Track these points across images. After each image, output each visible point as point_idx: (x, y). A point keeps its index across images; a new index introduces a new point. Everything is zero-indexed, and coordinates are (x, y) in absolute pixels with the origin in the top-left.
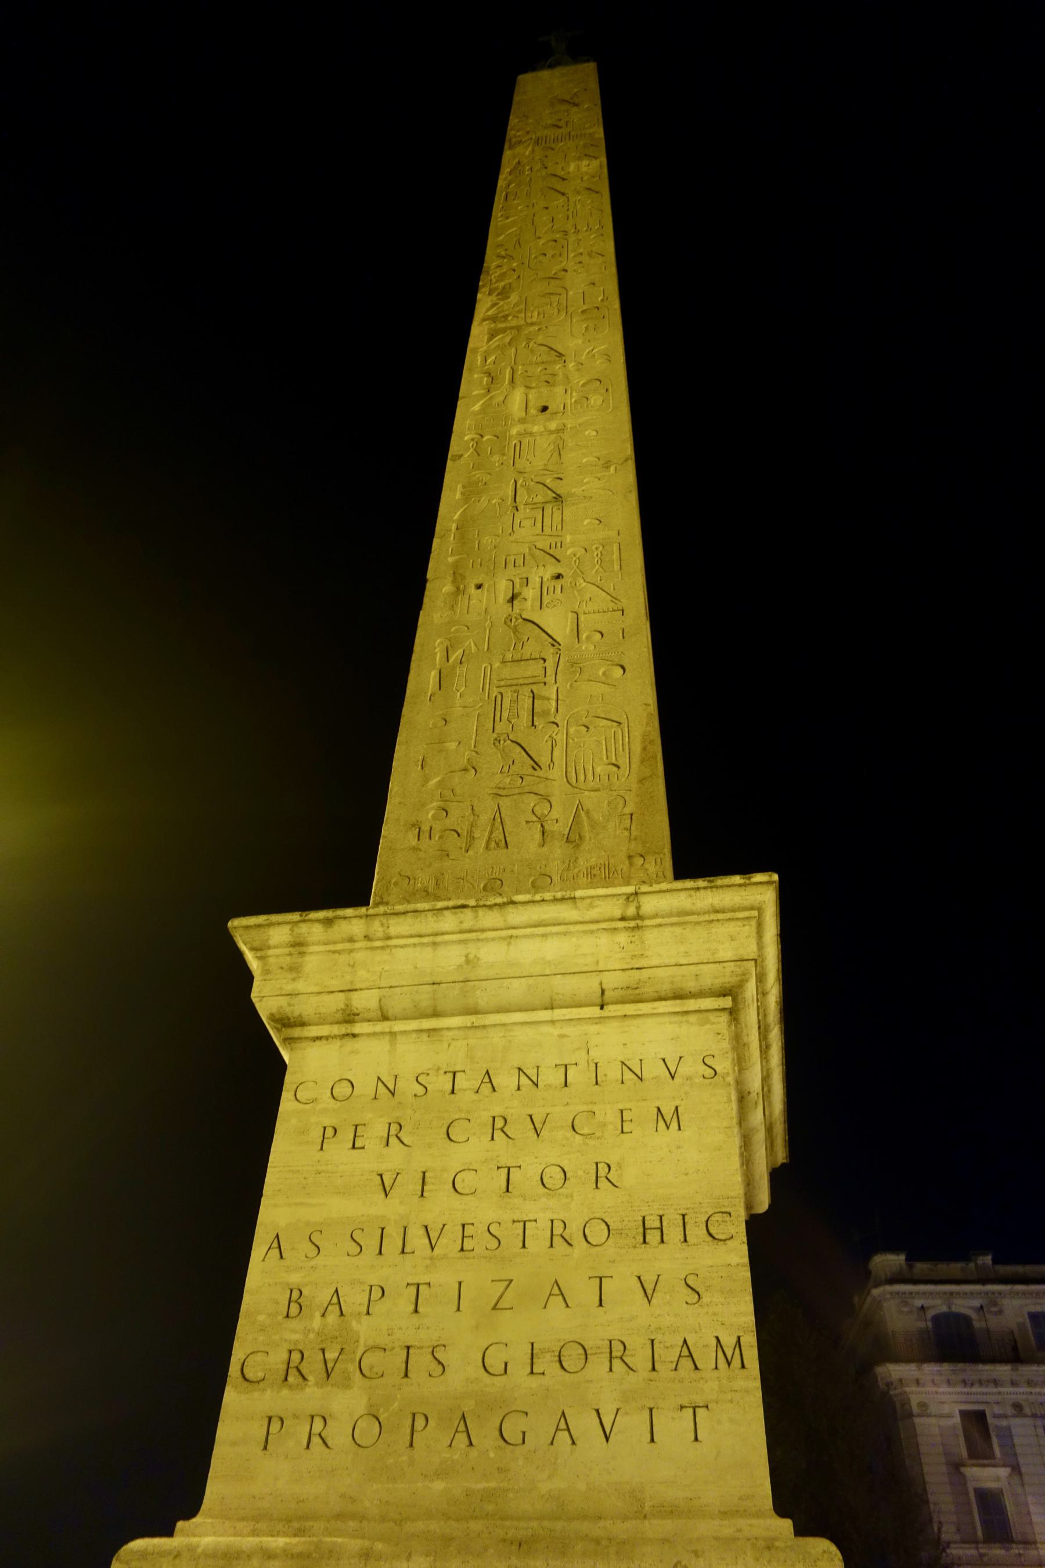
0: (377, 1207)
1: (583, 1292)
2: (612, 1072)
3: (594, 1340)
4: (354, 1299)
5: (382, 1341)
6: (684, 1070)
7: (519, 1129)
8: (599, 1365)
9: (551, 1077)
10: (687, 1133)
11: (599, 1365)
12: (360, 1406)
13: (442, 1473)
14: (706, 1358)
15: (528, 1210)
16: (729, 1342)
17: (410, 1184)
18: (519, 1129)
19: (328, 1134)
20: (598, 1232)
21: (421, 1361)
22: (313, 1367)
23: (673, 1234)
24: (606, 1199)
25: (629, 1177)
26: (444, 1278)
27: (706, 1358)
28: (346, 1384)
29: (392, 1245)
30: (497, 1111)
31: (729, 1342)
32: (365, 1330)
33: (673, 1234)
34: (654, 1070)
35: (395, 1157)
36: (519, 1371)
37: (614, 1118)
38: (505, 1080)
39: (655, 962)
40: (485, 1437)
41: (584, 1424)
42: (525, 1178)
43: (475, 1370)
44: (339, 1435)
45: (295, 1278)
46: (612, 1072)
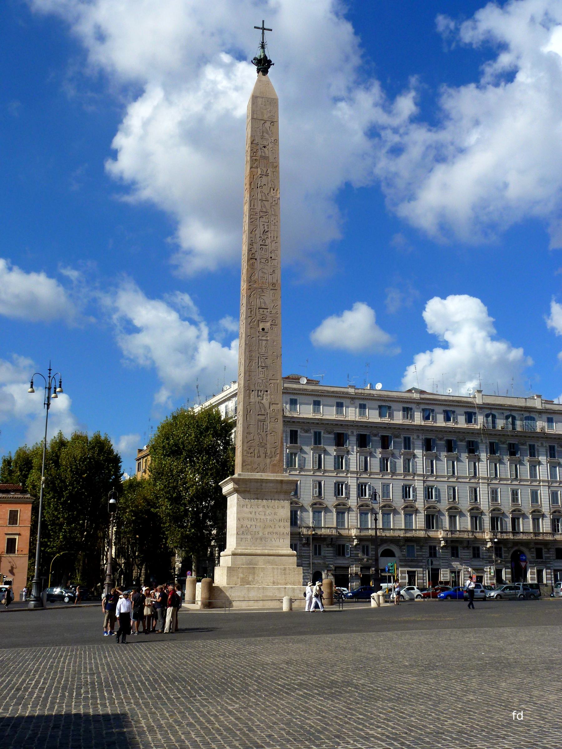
0: (250, 516)
3: (274, 532)
4: (249, 526)
7: (266, 507)
8: (275, 534)
11: (275, 534)
13: (259, 544)
14: (285, 534)
15: (267, 517)
17: (253, 513)
18: (266, 507)
19: (243, 506)
20: (275, 520)
21: (256, 533)
22: (245, 533)
23: (283, 521)
24: (276, 516)
26: (258, 524)
27: (285, 534)
29: (252, 520)
32: (251, 530)
33: (283, 521)
35: (251, 510)
41: (273, 540)
42: (267, 513)
44: (249, 540)
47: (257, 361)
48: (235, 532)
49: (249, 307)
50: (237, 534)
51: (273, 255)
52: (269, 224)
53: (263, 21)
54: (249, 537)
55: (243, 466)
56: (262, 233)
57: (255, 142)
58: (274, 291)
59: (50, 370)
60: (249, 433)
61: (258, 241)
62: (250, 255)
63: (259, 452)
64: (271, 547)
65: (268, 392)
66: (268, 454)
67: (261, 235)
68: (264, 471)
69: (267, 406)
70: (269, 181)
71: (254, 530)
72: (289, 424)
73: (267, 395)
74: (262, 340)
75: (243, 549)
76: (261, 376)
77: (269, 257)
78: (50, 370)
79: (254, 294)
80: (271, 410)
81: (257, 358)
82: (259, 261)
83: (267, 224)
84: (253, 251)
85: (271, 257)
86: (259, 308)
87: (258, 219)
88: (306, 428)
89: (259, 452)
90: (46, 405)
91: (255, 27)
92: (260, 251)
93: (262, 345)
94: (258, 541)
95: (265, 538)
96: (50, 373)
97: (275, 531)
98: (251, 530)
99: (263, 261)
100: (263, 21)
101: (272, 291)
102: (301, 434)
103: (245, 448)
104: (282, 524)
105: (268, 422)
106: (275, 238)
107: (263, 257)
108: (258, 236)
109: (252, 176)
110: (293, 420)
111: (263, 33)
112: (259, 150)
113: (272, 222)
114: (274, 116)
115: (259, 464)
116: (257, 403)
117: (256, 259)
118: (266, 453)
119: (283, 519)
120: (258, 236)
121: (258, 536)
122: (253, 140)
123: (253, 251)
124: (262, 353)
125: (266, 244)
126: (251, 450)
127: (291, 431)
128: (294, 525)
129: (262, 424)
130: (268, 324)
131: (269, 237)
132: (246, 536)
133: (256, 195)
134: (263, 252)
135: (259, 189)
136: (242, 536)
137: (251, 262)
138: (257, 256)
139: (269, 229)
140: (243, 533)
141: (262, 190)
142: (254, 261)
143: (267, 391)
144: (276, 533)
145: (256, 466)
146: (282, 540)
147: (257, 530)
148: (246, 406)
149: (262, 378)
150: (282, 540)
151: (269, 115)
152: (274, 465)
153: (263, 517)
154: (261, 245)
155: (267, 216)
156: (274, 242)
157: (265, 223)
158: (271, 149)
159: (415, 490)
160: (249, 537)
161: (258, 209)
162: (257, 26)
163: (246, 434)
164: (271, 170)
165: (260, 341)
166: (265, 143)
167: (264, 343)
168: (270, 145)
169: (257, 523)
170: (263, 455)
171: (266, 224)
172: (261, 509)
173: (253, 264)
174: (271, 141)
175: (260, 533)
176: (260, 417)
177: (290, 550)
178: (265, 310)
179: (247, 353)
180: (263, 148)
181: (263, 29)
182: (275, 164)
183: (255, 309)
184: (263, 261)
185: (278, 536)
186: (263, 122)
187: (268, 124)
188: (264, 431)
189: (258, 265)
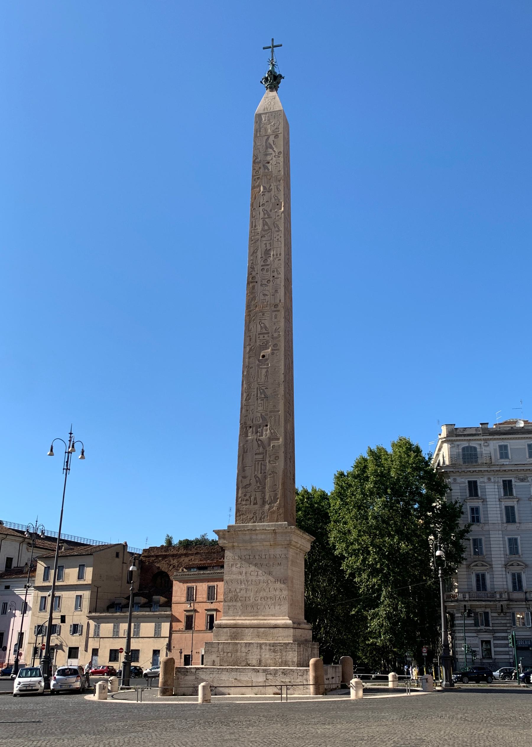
1: (267, 590)
2: (272, 556)
4: (238, 590)
5: (242, 596)
6: (282, 556)
8: (269, 600)
9: (264, 557)
10: (282, 567)
11: (269, 600)
12: (240, 604)
16: (285, 597)
19: (232, 565)
20: (269, 581)
21: (247, 599)
22: (234, 599)
25: (274, 574)
26: (249, 587)
28: (238, 602)
30: (256, 562)
31: (285, 597)
34: (278, 556)
36: (259, 600)
37: (272, 564)
38: (257, 557)
39: (278, 540)
40: (255, 609)
43: (254, 600)
45: (230, 587)
46: (272, 556)
47: (256, 392)
49: (248, 335)
51: (275, 274)
52: (271, 241)
55: (236, 516)
56: (263, 253)
57: (258, 160)
58: (276, 313)
59: (71, 434)
60: (244, 477)
61: (259, 262)
62: (251, 279)
63: (255, 499)
64: (264, 616)
65: (268, 427)
66: (267, 500)
67: (263, 255)
69: (266, 442)
70: (272, 196)
71: (245, 596)
72: (500, 473)
73: (267, 430)
74: (262, 368)
75: (229, 620)
76: (260, 408)
77: (272, 276)
78: (71, 434)
79: (254, 320)
80: (271, 446)
81: (256, 389)
82: (259, 283)
83: (269, 242)
84: (254, 274)
85: (274, 277)
86: (259, 334)
87: (260, 239)
88: (521, 476)
89: (255, 499)
90: (65, 470)
91: (264, 48)
92: (261, 272)
93: (261, 373)
94: (249, 609)
95: (257, 604)
96: (70, 437)
97: (270, 595)
98: (239, 594)
99: (265, 282)
101: (274, 313)
102: (516, 484)
103: (240, 495)
105: (267, 461)
106: (278, 255)
107: (263, 278)
108: (259, 256)
109: (254, 196)
110: (504, 469)
111: (273, 51)
112: (262, 168)
113: (274, 239)
114: (278, 128)
115: (255, 513)
116: (255, 440)
117: (257, 282)
118: (264, 498)
119: (279, 580)
120: (259, 256)
121: (248, 602)
122: (256, 159)
123: (254, 274)
124: (261, 383)
125: (268, 263)
126: (247, 497)
127: (504, 481)
128: (519, 590)
129: (260, 464)
131: (272, 256)
132: (234, 603)
133: (258, 214)
134: (265, 272)
135: (261, 208)
136: (230, 604)
137: (251, 285)
138: (258, 278)
139: (272, 247)
140: (231, 600)
141: (264, 207)
142: (255, 284)
143: (267, 426)
144: (271, 598)
145: (251, 515)
146: (277, 607)
147: (248, 595)
148: (241, 445)
149: (261, 411)
150: (277, 607)
151: (273, 128)
152: (273, 513)
153: (254, 578)
154: (262, 266)
155: (269, 234)
156: (277, 259)
157: (267, 242)
158: (275, 163)
160: (239, 604)
161: (259, 228)
162: (266, 46)
163: (240, 478)
164: (275, 183)
165: (259, 370)
166: (269, 158)
167: (264, 371)
168: (274, 158)
169: (248, 585)
170: (259, 501)
171: (268, 242)
173: (253, 287)
174: (274, 155)
175: (251, 598)
176: (257, 457)
177: (287, 619)
178: (266, 336)
179: (245, 386)
180: (267, 165)
182: (278, 177)
183: (254, 337)
185: (273, 602)
186: (266, 137)
187: (272, 138)
188: (262, 472)
189: (258, 287)
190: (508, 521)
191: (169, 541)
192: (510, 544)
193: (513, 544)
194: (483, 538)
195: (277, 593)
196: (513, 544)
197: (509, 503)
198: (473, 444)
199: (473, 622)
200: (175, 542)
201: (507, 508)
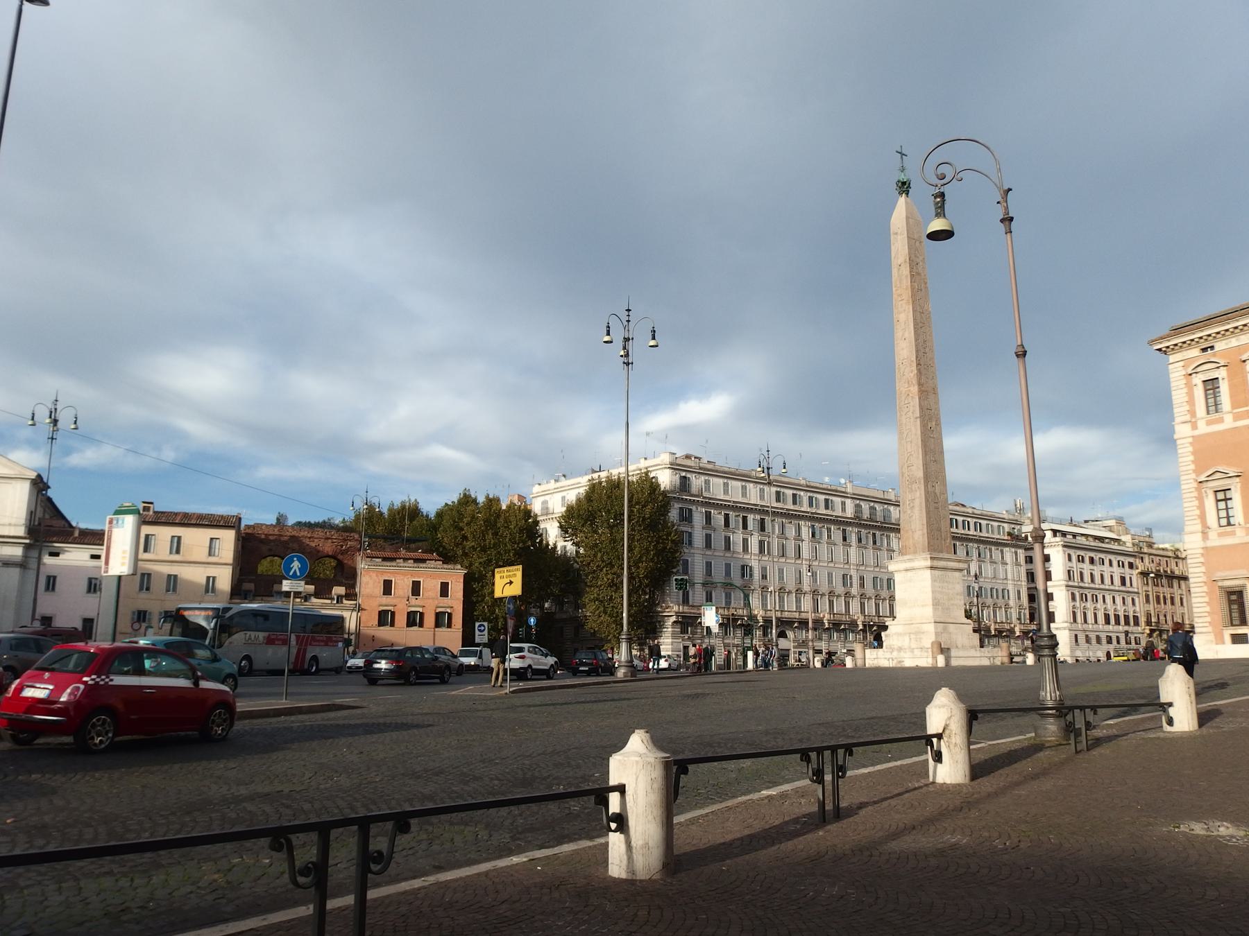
48: (931, 603)
50: (933, 605)
53: (901, 147)
54: (940, 608)
68: (941, 552)
99: (926, 366)
100: (901, 147)
104: (959, 597)
111: (902, 157)
130: (934, 423)
140: (936, 605)
153: (947, 591)
159: (851, 576)
172: (946, 584)
181: (902, 154)
184: (926, 366)
190: (706, 547)
191: (281, 520)
192: (707, 566)
193: (709, 565)
194: (690, 560)
195: (959, 601)
196: (709, 565)
197: (709, 532)
198: (688, 475)
199: (679, 630)
200: (291, 522)
201: (706, 535)
